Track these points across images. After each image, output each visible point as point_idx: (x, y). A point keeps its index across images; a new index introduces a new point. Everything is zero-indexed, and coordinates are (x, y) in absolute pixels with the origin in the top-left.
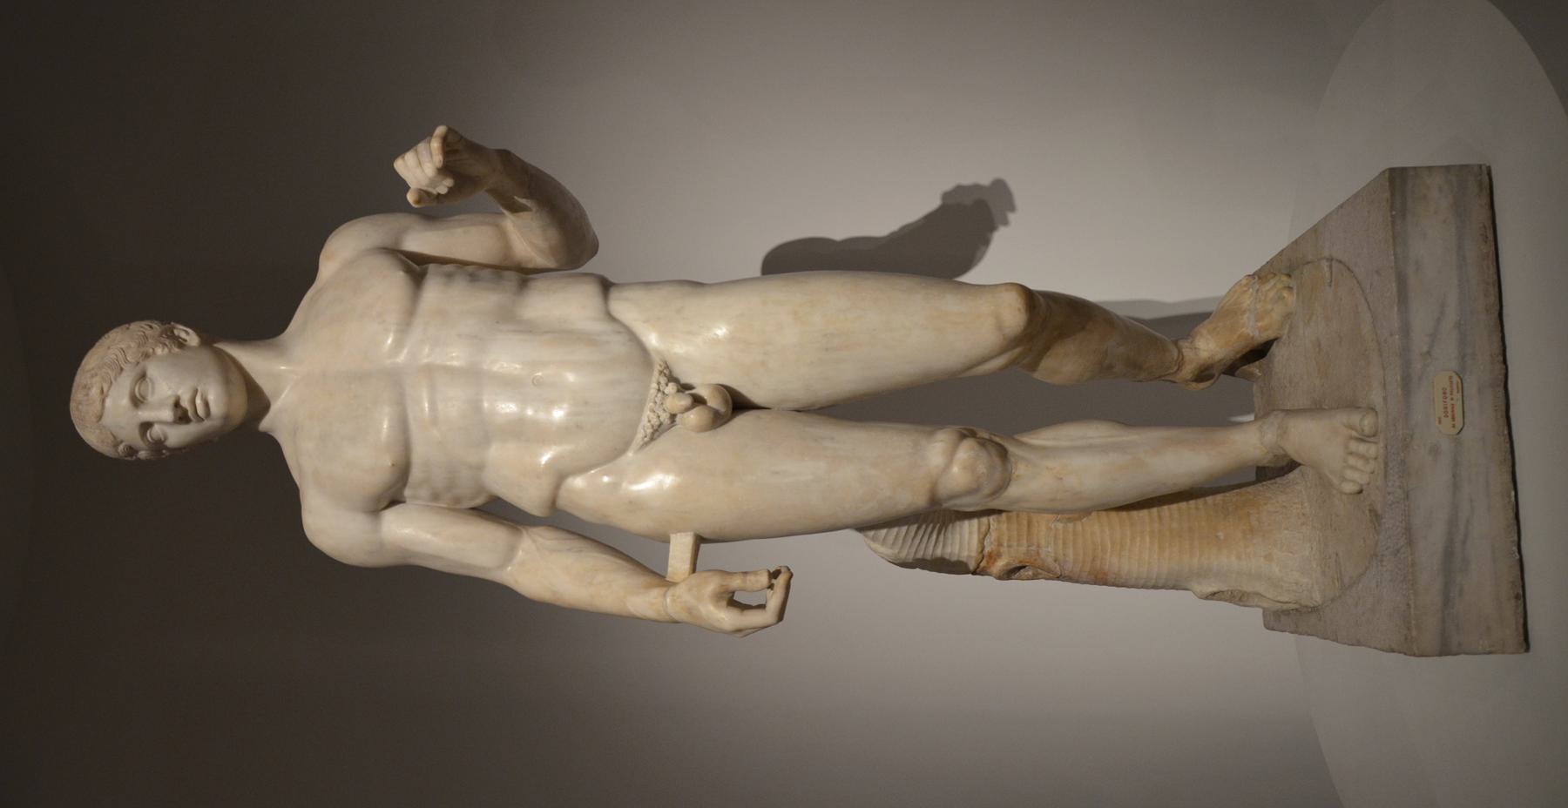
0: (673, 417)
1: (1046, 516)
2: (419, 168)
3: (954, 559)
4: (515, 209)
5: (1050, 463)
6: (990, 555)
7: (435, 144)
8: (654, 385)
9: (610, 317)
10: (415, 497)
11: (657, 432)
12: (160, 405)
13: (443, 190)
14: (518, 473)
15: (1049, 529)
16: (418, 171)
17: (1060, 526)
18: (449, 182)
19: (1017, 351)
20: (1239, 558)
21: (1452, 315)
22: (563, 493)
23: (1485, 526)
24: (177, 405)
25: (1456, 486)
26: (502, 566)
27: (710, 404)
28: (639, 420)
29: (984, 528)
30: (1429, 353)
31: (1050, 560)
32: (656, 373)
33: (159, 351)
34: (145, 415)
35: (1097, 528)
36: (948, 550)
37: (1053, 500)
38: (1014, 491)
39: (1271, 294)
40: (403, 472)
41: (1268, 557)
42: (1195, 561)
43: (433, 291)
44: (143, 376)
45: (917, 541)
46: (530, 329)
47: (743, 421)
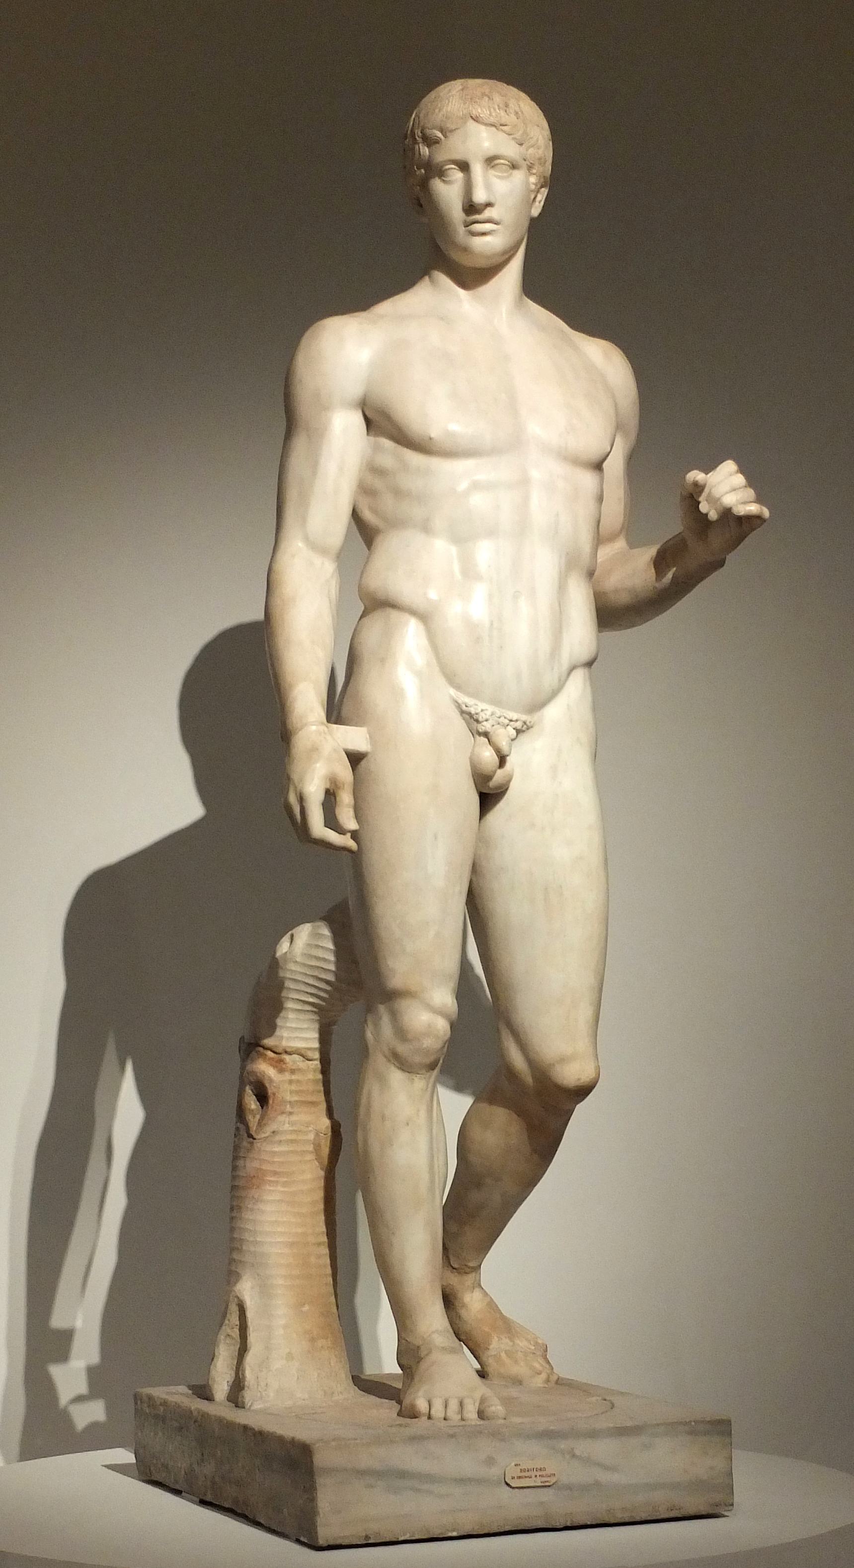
1: (326, 1122)
2: (727, 487)
3: (279, 1022)
4: (660, 563)
5: (423, 1114)
6: (282, 1061)
7: (753, 508)
8: (514, 716)
9: (572, 668)
10: (377, 448)
11: (471, 718)
12: (488, 187)
13: (704, 507)
14: (419, 565)
15: (308, 1125)
16: (727, 488)
17: (311, 1136)
18: (713, 515)
19: (529, 1080)
20: (285, 1327)
21: (605, 1477)
22: (406, 617)
23: (427, 1509)
24: (489, 205)
25: (461, 1481)
27: (499, 772)
29: (310, 1054)
30: (574, 1456)
31: (273, 1126)
32: (524, 717)
33: (533, 179)
35: (308, 1176)
36: (291, 1015)
37: (383, 1118)
38: (396, 1077)
39: (537, 1365)
40: (403, 438)
41: (290, 1357)
42: (280, 1281)
43: (588, 480)
44: (514, 166)
45: (311, 981)
46: (562, 588)
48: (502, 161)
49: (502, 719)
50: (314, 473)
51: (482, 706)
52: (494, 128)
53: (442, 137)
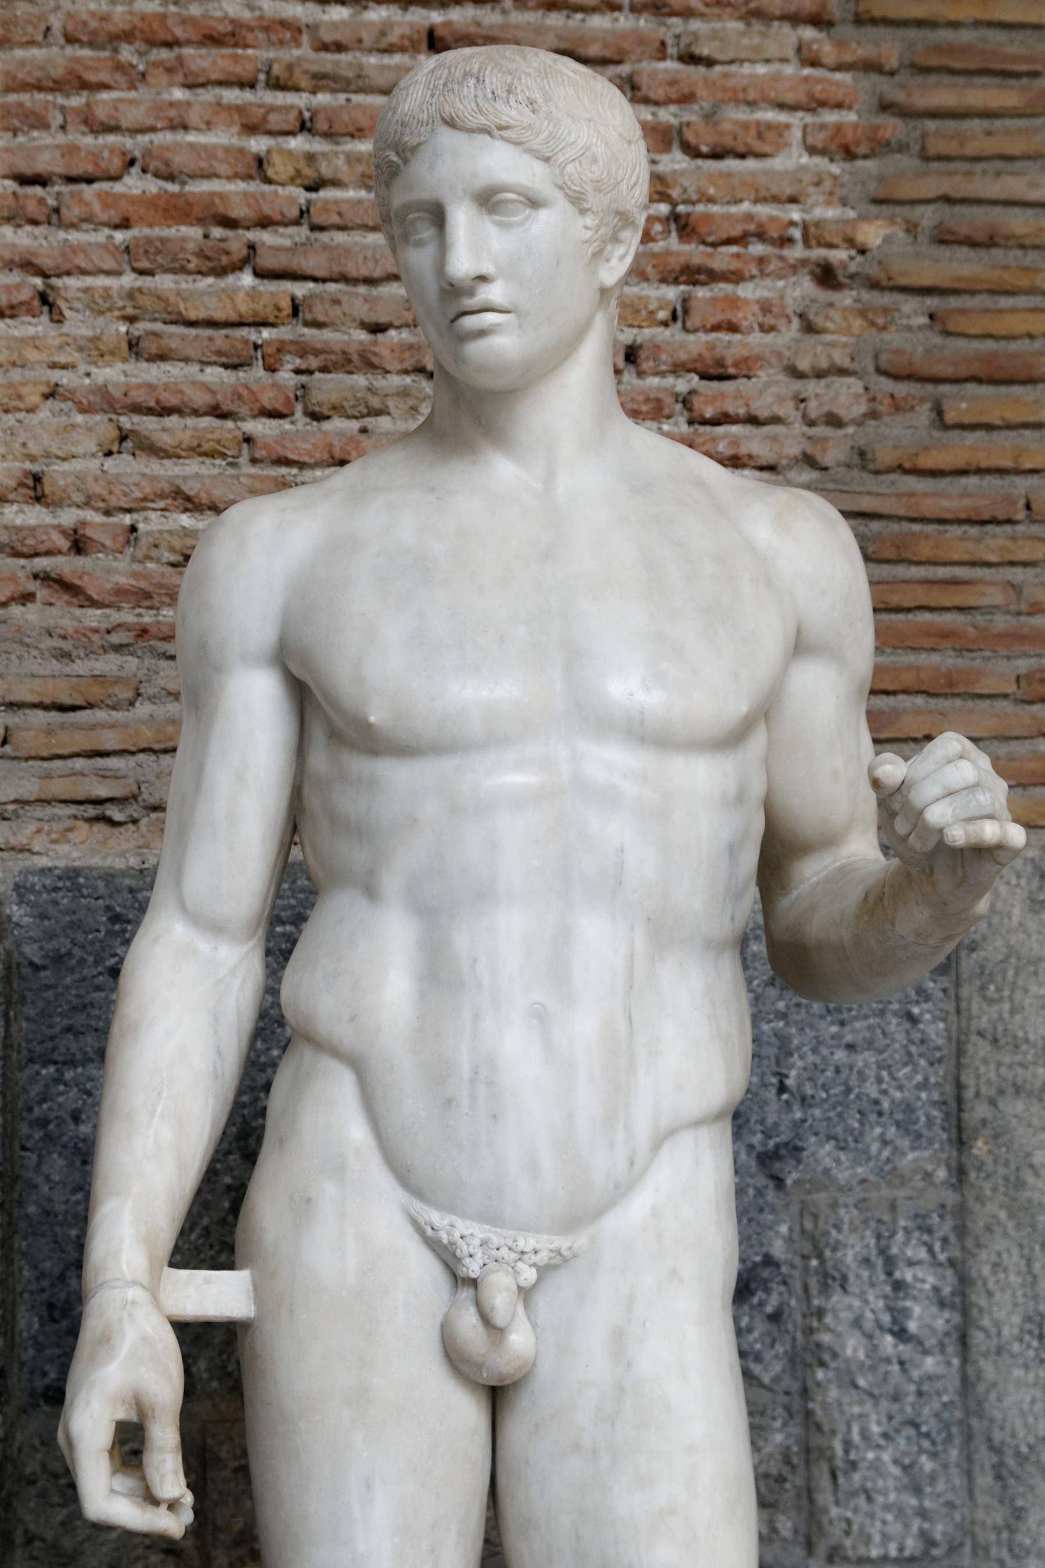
0: (474, 1283)
22: (329, 1064)
24: (482, 279)
26: (183, 907)
28: (464, 1215)
34: (462, 218)
47: (468, 1412)
48: (512, 196)
49: (504, 1252)
50: (198, 788)
51: (463, 1226)
52: (486, 137)
53: (400, 162)
